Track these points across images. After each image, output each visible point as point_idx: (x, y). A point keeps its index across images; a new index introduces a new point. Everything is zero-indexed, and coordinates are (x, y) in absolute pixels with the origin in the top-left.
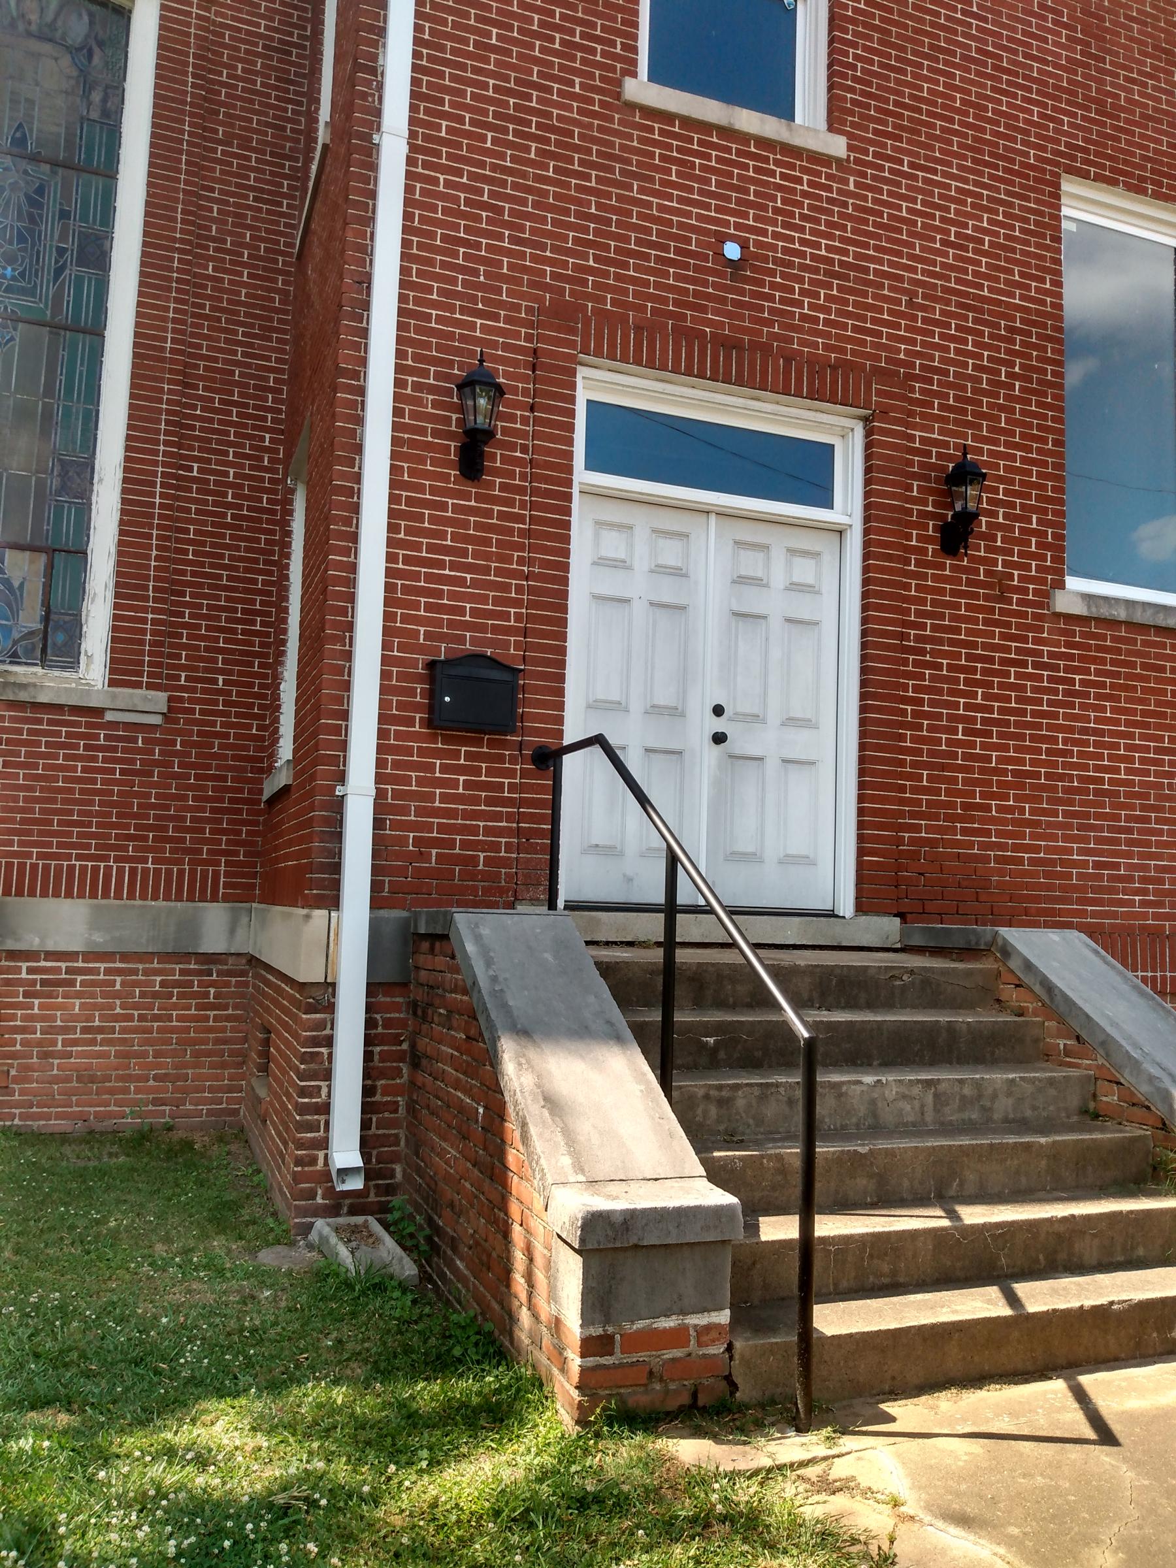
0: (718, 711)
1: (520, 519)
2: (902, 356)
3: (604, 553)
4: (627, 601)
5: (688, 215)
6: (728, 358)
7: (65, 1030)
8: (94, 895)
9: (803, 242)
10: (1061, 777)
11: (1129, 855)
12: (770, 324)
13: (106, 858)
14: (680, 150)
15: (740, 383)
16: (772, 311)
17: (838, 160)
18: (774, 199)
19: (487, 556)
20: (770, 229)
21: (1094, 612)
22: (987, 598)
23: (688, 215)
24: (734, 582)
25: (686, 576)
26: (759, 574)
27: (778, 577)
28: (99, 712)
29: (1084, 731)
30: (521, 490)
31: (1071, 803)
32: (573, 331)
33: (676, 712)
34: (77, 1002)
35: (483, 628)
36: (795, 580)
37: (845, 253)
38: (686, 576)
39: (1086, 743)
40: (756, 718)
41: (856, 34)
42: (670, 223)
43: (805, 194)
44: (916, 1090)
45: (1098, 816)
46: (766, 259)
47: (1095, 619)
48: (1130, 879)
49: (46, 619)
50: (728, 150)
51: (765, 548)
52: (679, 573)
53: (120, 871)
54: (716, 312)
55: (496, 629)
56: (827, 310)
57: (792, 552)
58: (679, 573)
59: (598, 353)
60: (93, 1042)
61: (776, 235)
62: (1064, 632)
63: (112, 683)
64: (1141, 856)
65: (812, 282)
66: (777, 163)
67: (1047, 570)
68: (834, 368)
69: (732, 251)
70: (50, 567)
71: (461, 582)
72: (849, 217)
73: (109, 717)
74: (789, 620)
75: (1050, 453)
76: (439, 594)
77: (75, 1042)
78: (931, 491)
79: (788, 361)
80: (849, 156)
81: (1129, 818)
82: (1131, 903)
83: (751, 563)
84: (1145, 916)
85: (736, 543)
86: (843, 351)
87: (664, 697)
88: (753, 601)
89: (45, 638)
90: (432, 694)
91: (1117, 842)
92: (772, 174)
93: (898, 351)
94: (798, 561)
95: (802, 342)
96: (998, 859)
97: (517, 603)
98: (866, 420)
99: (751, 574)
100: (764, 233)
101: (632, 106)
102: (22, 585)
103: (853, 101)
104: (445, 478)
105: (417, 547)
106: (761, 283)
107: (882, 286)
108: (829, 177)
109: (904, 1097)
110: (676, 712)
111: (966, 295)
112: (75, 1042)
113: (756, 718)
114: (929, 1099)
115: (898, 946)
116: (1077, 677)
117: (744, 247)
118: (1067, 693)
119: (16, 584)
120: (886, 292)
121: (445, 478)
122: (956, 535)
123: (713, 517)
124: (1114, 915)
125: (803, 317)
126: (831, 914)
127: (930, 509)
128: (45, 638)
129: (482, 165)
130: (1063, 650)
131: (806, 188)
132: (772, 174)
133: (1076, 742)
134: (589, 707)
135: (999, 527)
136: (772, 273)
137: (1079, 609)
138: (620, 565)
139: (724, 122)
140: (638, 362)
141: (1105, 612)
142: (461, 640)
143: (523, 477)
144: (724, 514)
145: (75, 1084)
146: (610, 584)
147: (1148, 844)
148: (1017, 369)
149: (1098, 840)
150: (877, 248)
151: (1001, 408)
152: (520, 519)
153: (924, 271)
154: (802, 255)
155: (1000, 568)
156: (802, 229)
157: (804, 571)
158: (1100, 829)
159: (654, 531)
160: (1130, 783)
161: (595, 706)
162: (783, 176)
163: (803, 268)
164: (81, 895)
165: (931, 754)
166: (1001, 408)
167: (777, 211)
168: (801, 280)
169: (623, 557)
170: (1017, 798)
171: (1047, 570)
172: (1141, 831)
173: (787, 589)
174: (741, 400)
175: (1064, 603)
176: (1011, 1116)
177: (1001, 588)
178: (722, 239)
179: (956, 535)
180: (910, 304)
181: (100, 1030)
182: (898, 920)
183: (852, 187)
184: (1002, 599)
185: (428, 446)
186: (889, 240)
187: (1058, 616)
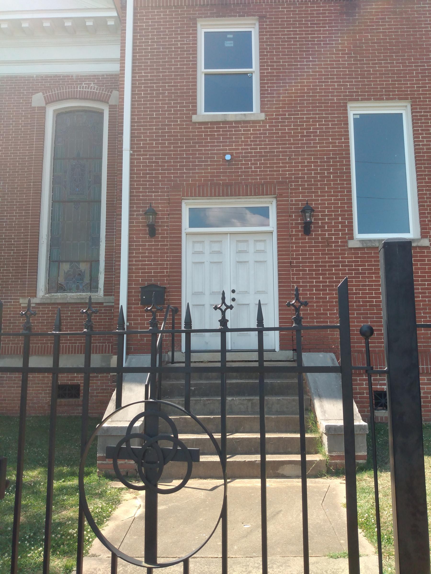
0: (233, 291)
1: (167, 245)
2: (287, 176)
3: (196, 250)
4: (204, 263)
5: (214, 150)
6: (227, 189)
7: (96, 389)
8: (102, 353)
9: (251, 149)
12: (241, 176)
13: (105, 343)
14: (210, 132)
15: (231, 195)
16: (241, 172)
17: (263, 121)
18: (241, 138)
19: (158, 257)
20: (240, 147)
21: (365, 245)
22: (322, 246)
23: (214, 150)
24: (237, 253)
25: (221, 253)
26: (245, 249)
27: (251, 249)
28: (102, 303)
30: (167, 237)
32: (180, 192)
34: (99, 382)
35: (157, 276)
36: (258, 249)
37: (266, 148)
38: (221, 253)
40: (246, 292)
41: (267, 80)
42: (208, 154)
43: (251, 134)
44: (245, 402)
46: (239, 157)
47: (366, 248)
49: (91, 280)
50: (226, 127)
51: (247, 241)
52: (219, 252)
53: (109, 346)
54: (223, 176)
55: (160, 276)
56: (260, 168)
57: (256, 241)
58: (219, 252)
59: (187, 196)
60: (103, 393)
61: (242, 149)
63: (105, 295)
65: (255, 160)
66: (242, 127)
67: (346, 234)
68: (263, 185)
69: (228, 157)
70: (91, 266)
71: (151, 265)
72: (267, 137)
73: (105, 304)
74: (256, 262)
75: (346, 195)
76: (144, 269)
77: (99, 393)
78: (299, 216)
79: (247, 186)
80: (266, 119)
83: (242, 247)
85: (237, 241)
86: (267, 179)
88: (243, 257)
89: (91, 285)
90: (142, 296)
92: (240, 131)
93: (286, 174)
94: (258, 244)
95: (252, 179)
97: (167, 268)
98: (276, 198)
99: (243, 249)
100: (238, 149)
101: (195, 123)
102: (84, 271)
103: (267, 101)
104: (146, 238)
105: (138, 257)
106: (238, 165)
107: (279, 156)
108: (259, 126)
109: (241, 404)
111: (311, 151)
112: (99, 393)
113: (246, 292)
114: (250, 404)
115: (292, 360)
116: (360, 268)
117: (232, 155)
119: (83, 271)
120: (281, 157)
121: (146, 238)
122: (307, 229)
123: (229, 235)
125: (252, 172)
126: (274, 351)
127: (299, 221)
128: (91, 285)
129: (153, 151)
130: (354, 259)
131: (252, 132)
132: (240, 131)
133: (360, 290)
134: (193, 294)
135: (326, 223)
136: (242, 161)
137: (358, 245)
138: (201, 253)
139: (223, 120)
140: (199, 196)
141: (369, 245)
142: (151, 280)
143: (167, 234)
144: (231, 233)
145: (99, 404)
146: (198, 259)
148: (331, 171)
150: (277, 144)
151: (325, 185)
152: (167, 245)
153: (294, 148)
154: (251, 153)
155: (327, 236)
156: (251, 145)
157: (260, 246)
159: (211, 241)
161: (195, 294)
162: (244, 131)
163: (252, 157)
164: (99, 353)
166: (325, 185)
167: (242, 142)
168: (251, 160)
169: (201, 250)
171: (346, 234)
173: (255, 252)
174: (234, 200)
175: (351, 244)
176: (279, 410)
177: (328, 242)
178: (225, 154)
179: (307, 229)
180: (290, 159)
181: (105, 389)
182: (292, 352)
183: (268, 127)
184: (328, 246)
185: (141, 230)
186: (281, 141)
187: (351, 249)
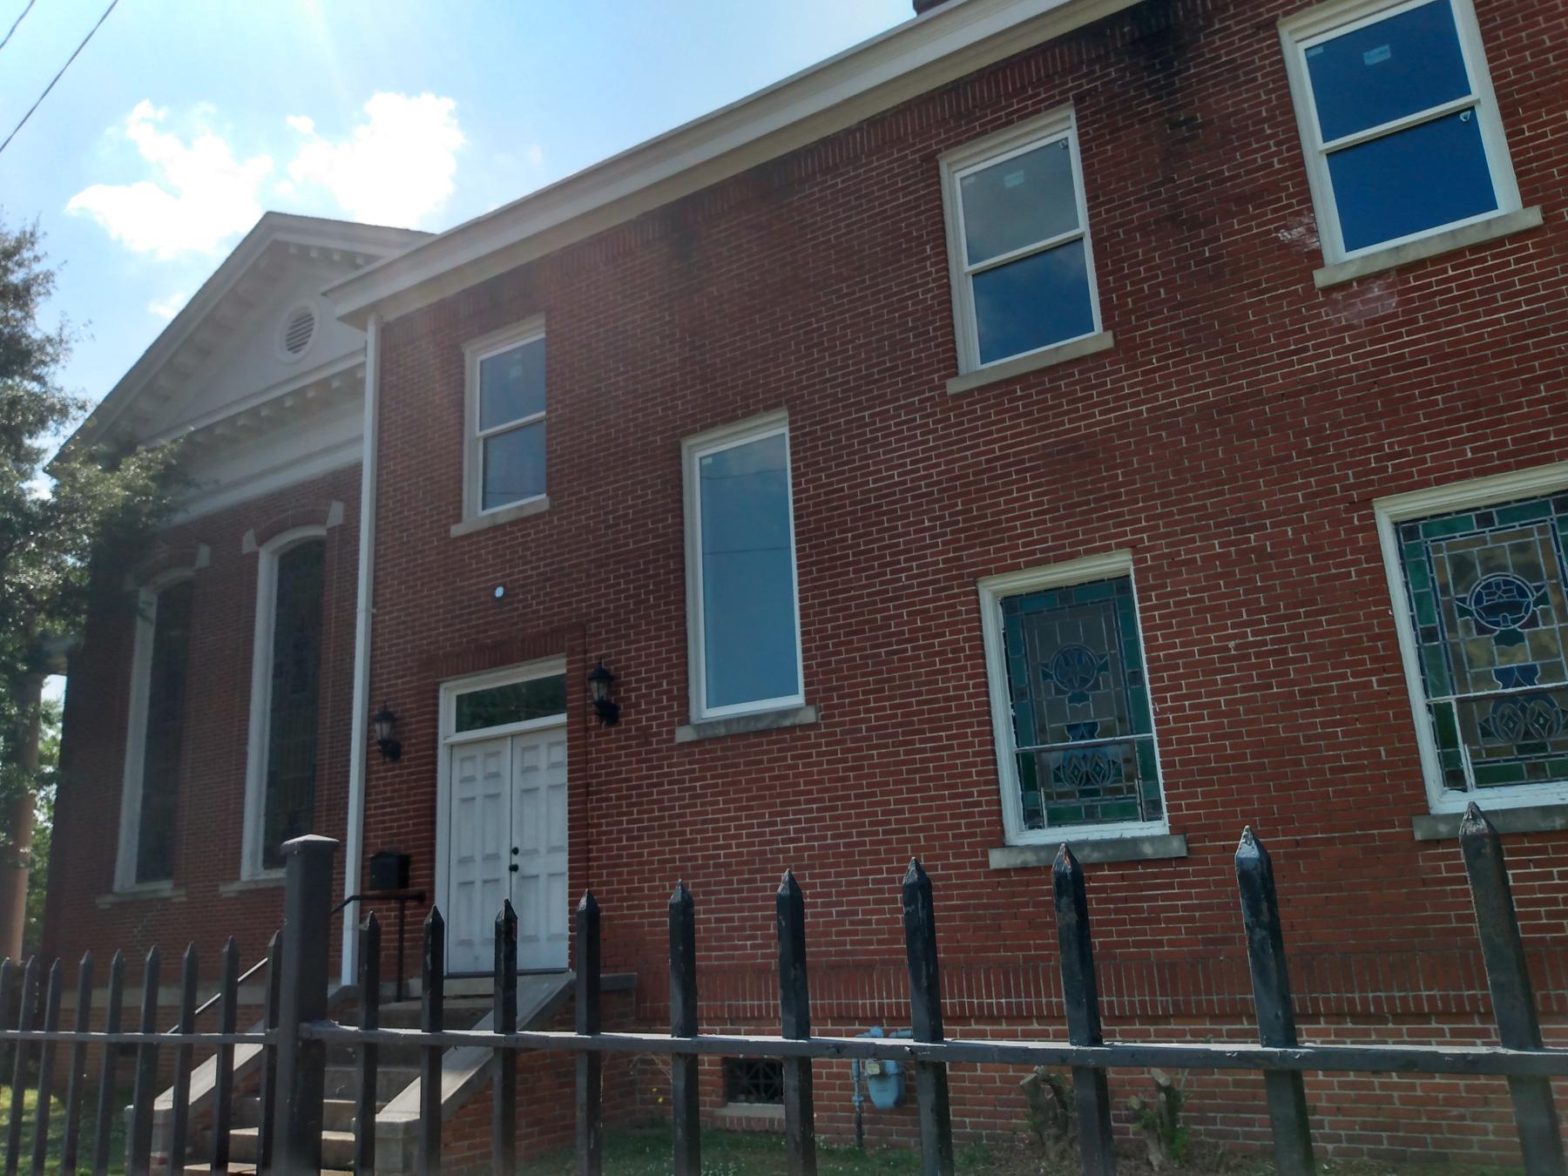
0: (515, 851)
10: (690, 859)
11: (741, 910)
29: (705, 822)
31: (697, 876)
33: (495, 857)
39: (706, 831)
40: (535, 851)
45: (717, 883)
48: (742, 928)
62: (688, 755)
64: (751, 909)
81: (739, 881)
82: (744, 947)
84: (754, 956)
87: (490, 849)
91: (732, 901)
96: (651, 925)
110: (495, 857)
113: (534, 852)
118: (691, 797)
122: (609, 713)
124: (732, 957)
147: (755, 899)
149: (718, 902)
158: (719, 892)
160: (740, 854)
165: (609, 858)
170: (661, 879)
172: (749, 890)
177: (645, 735)
